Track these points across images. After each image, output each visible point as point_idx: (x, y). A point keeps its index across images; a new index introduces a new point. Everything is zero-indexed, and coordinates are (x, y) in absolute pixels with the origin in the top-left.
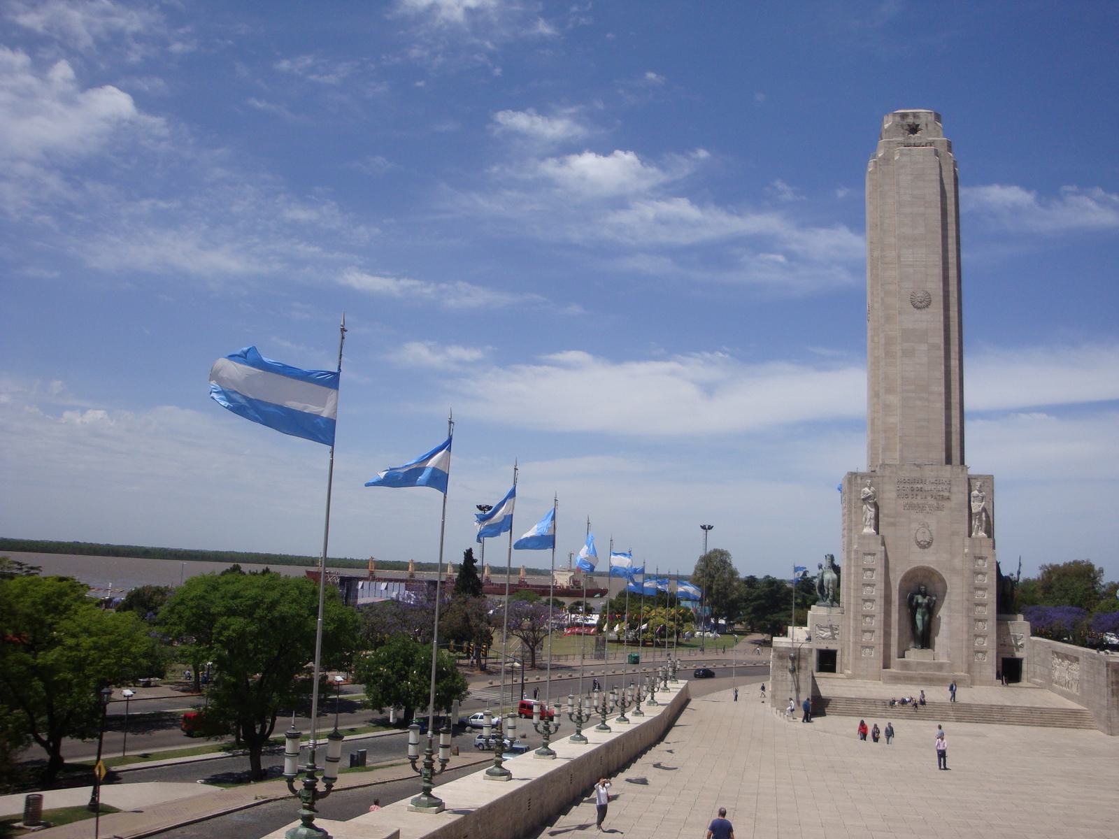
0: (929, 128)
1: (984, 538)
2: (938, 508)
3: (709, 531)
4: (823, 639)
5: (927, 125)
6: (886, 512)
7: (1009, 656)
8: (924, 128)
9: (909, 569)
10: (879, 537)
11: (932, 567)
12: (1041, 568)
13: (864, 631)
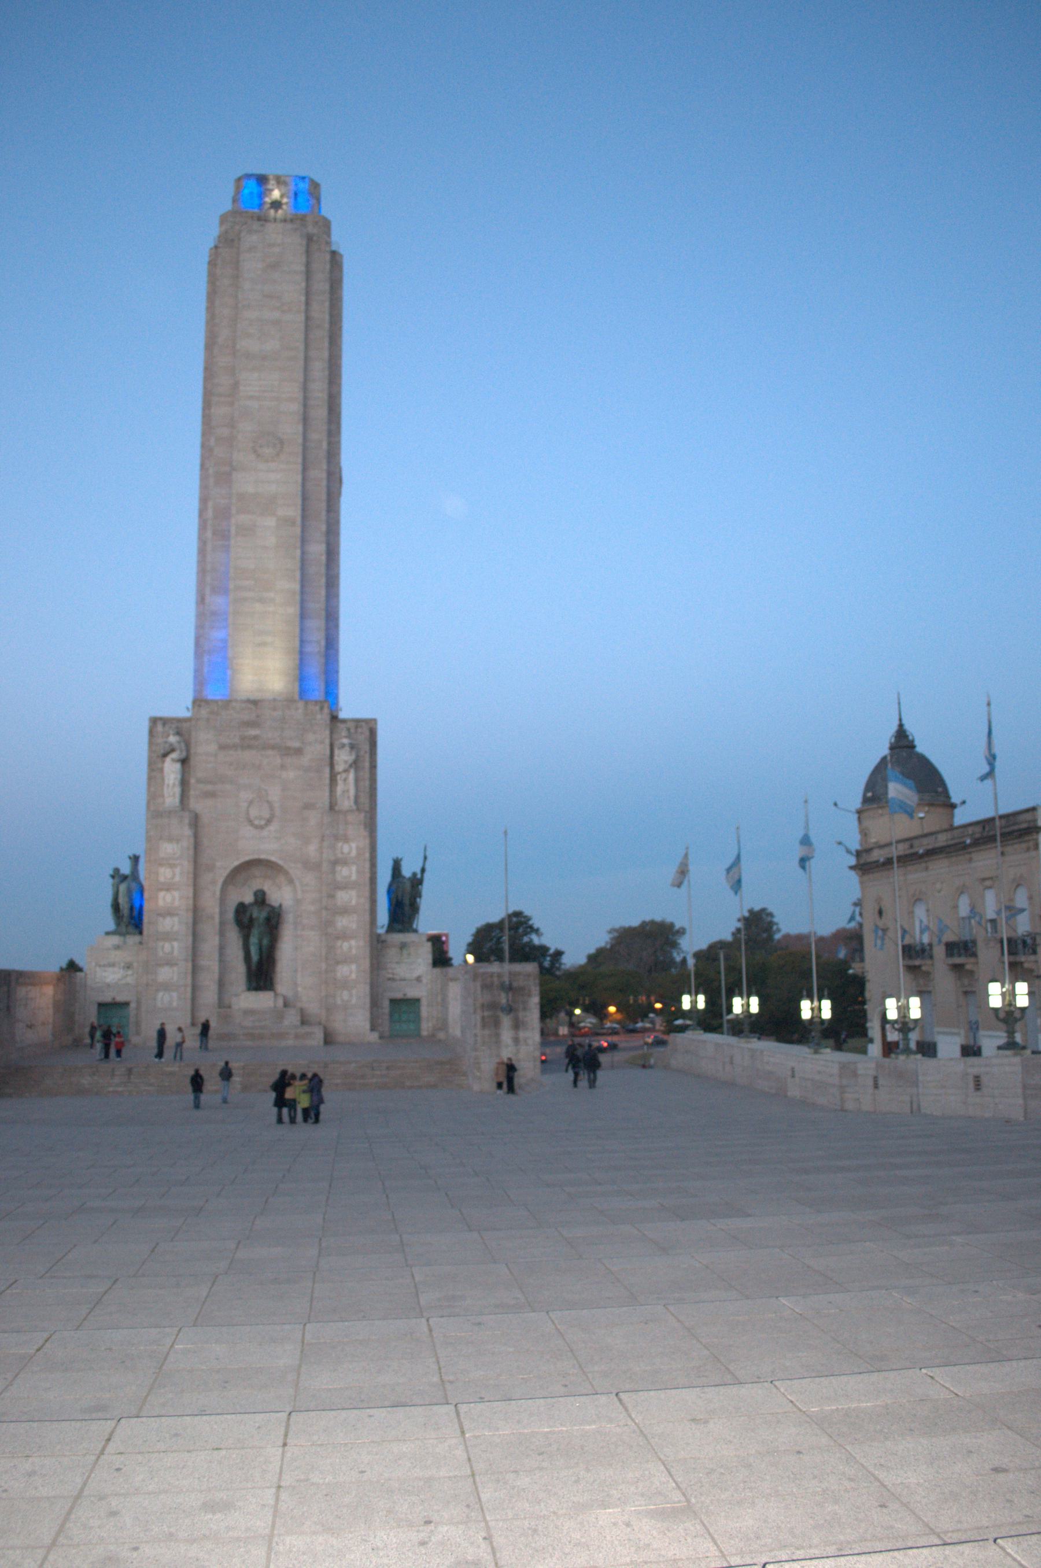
0: (300, 199)
1: (352, 811)
2: (283, 767)
4: (108, 985)
7: (399, 995)
9: (236, 863)
10: (186, 814)
11: (273, 859)
13: (160, 965)
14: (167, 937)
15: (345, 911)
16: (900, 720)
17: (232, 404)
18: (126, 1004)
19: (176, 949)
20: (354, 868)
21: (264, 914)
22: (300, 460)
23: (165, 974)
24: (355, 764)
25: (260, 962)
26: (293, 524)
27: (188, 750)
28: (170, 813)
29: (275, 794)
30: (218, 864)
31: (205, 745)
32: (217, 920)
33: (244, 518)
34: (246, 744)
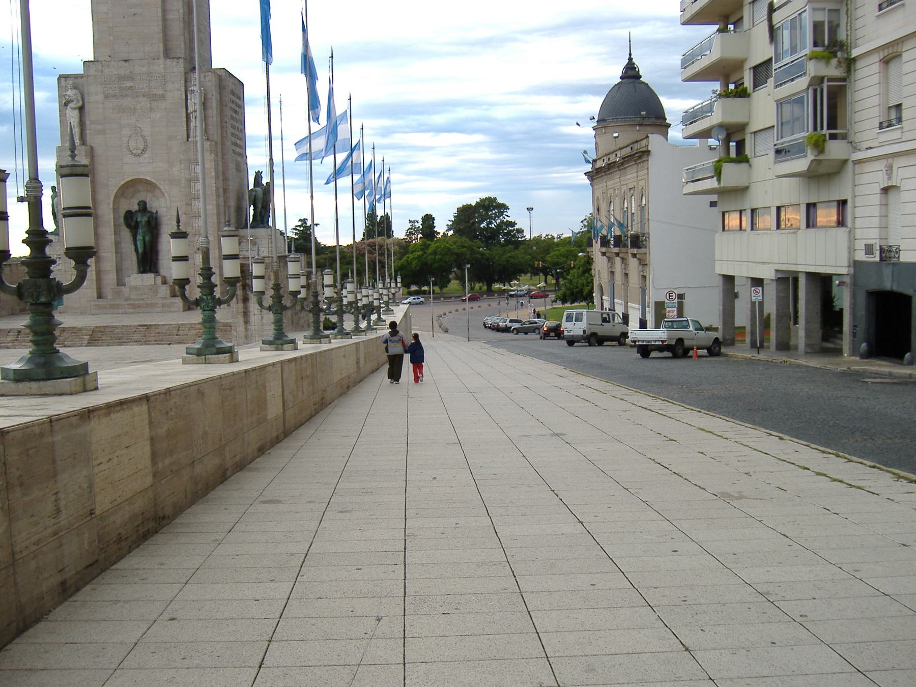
16: (630, 54)
21: (145, 219)
25: (145, 252)
27: (83, 100)
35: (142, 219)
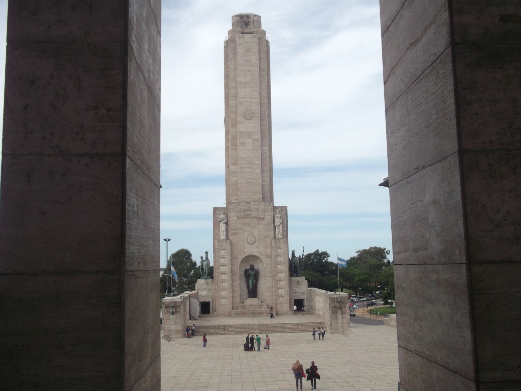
0: (255, 23)
3: (169, 242)
4: (203, 296)
5: (253, 22)
6: (231, 227)
7: (297, 298)
8: (252, 24)
12: (357, 252)
13: (222, 290)
14: (223, 281)
15: (280, 272)
17: (236, 99)
18: (208, 303)
19: (226, 285)
20: (283, 258)
21: (254, 273)
22: (259, 119)
23: (223, 293)
24: (282, 223)
26: (258, 141)
27: (227, 220)
28: (223, 240)
29: (256, 233)
30: (238, 256)
31: (233, 217)
32: (239, 275)
33: (242, 140)
34: (246, 217)
35: (252, 273)
